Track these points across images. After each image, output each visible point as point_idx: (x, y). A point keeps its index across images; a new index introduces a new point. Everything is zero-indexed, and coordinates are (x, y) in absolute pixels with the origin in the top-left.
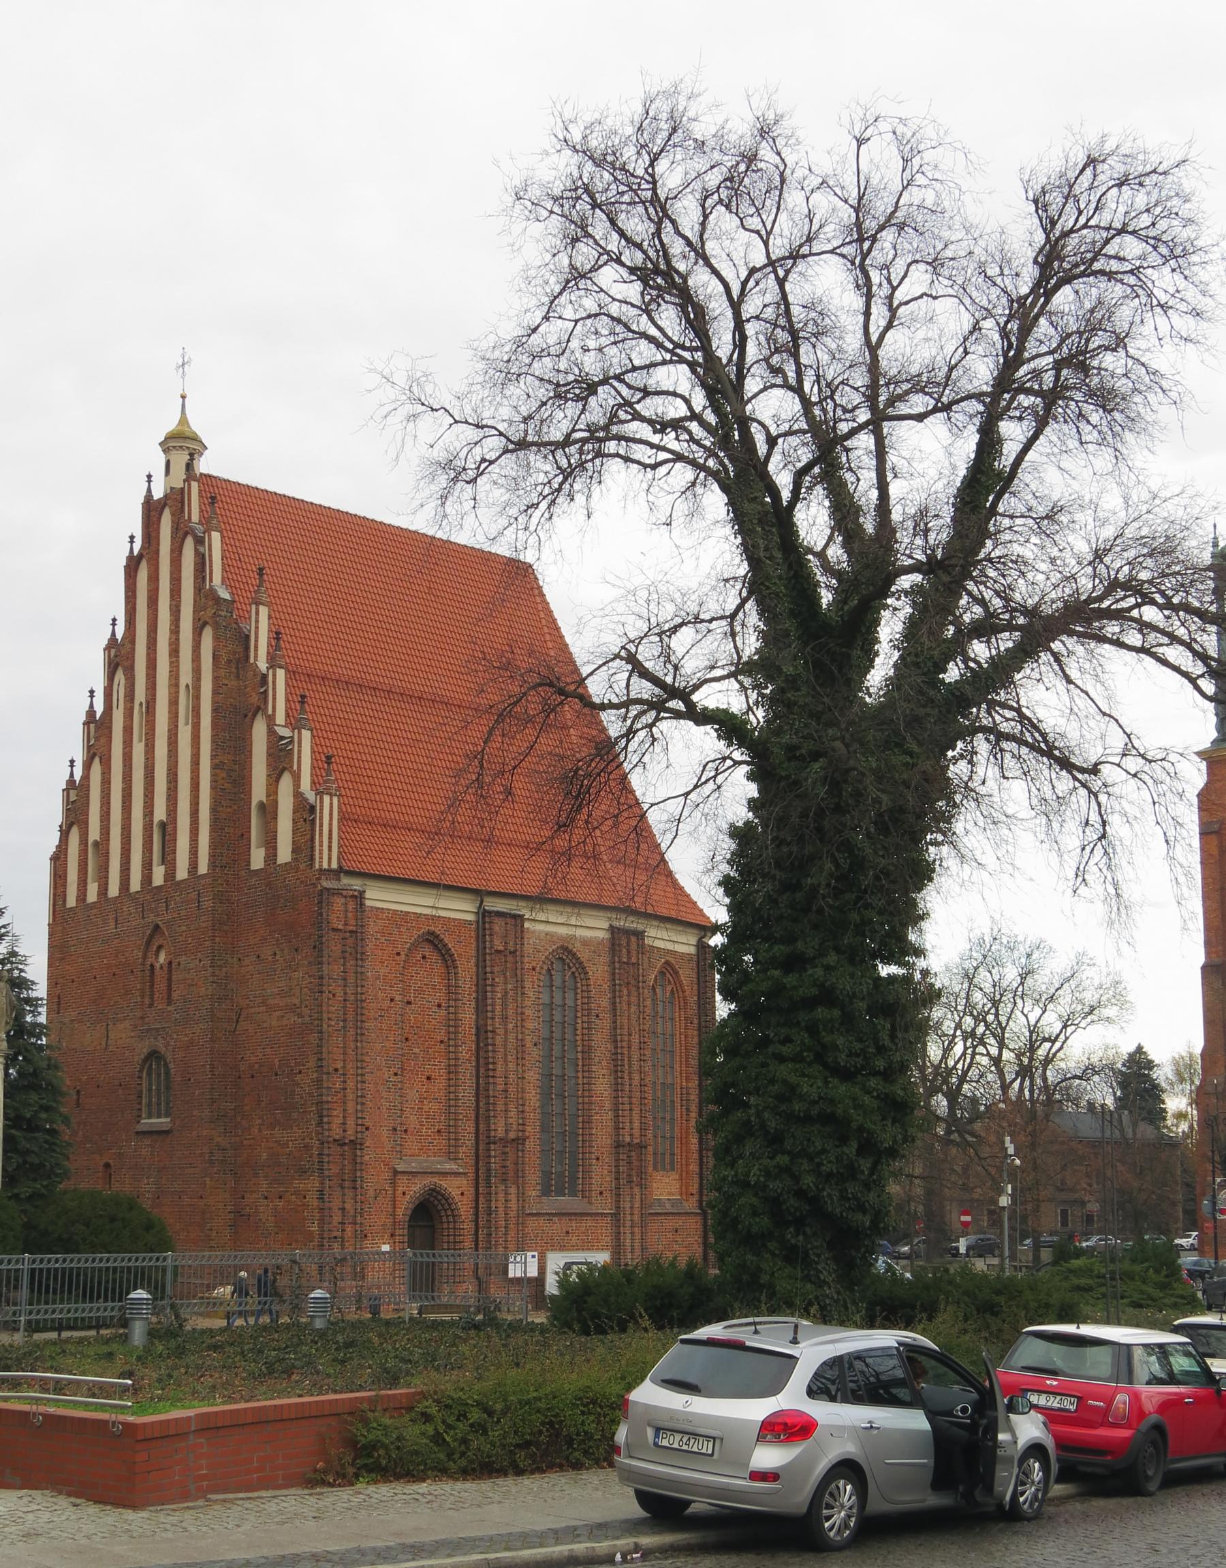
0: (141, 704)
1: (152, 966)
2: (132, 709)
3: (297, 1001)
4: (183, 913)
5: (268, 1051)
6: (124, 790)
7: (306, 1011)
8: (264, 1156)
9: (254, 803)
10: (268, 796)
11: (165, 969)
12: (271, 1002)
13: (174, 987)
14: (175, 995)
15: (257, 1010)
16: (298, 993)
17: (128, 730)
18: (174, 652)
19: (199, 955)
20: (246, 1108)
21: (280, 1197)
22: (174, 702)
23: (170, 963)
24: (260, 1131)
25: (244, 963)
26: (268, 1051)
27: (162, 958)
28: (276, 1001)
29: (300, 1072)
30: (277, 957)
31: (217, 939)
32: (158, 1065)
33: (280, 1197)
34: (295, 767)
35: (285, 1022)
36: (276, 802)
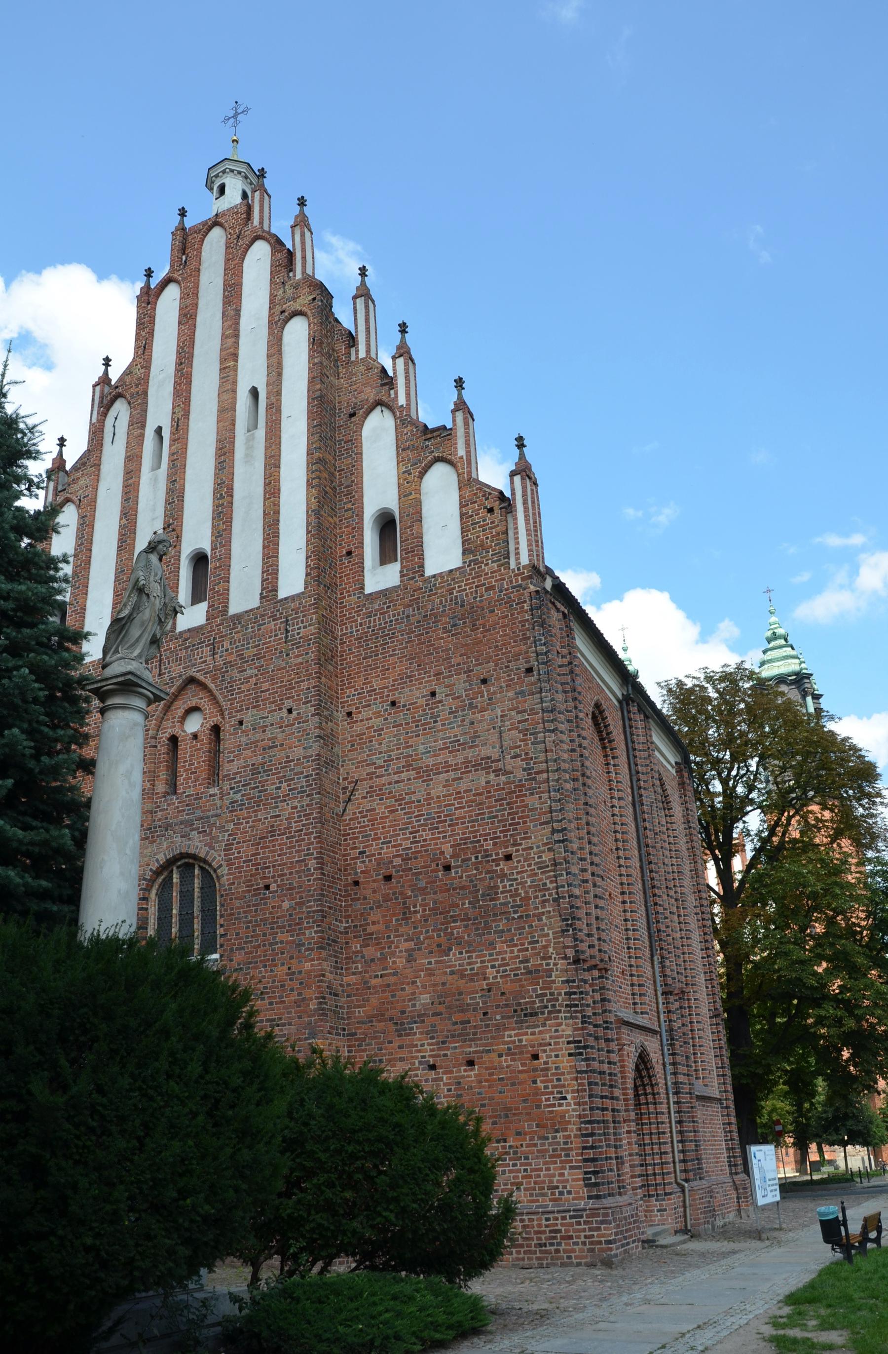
0: (159, 430)
1: (174, 740)
2: (142, 436)
3: (485, 751)
4: (249, 653)
5: (427, 835)
6: (122, 527)
7: (510, 763)
8: (425, 998)
9: (370, 511)
10: (403, 494)
11: (204, 738)
12: (431, 761)
13: (224, 757)
14: (228, 768)
15: (396, 777)
16: (494, 738)
17: (133, 461)
18: (229, 357)
19: (288, 703)
20: (371, 929)
21: (471, 1063)
22: (226, 412)
23: (216, 730)
24: (410, 959)
25: (364, 714)
26: (427, 835)
27: (194, 724)
28: (439, 759)
29: (508, 857)
30: (438, 697)
31: (323, 679)
32: (188, 877)
33: (471, 1063)
34: (461, 452)
35: (463, 786)
36: (418, 503)
